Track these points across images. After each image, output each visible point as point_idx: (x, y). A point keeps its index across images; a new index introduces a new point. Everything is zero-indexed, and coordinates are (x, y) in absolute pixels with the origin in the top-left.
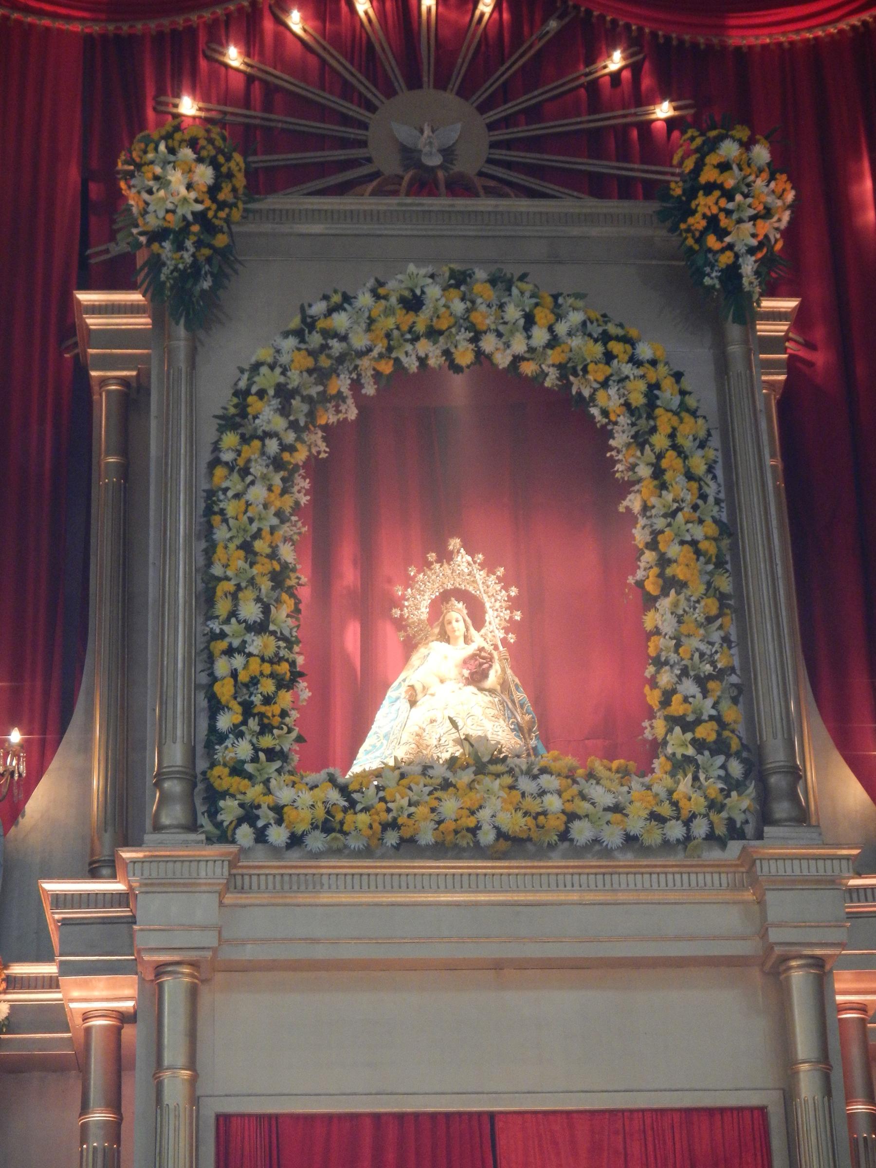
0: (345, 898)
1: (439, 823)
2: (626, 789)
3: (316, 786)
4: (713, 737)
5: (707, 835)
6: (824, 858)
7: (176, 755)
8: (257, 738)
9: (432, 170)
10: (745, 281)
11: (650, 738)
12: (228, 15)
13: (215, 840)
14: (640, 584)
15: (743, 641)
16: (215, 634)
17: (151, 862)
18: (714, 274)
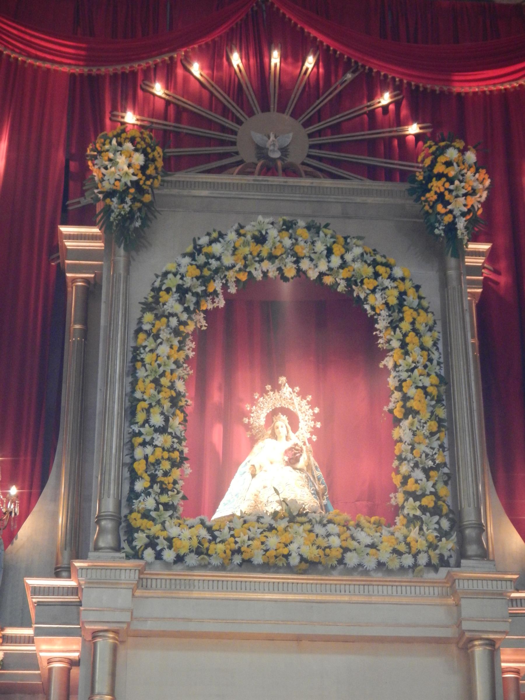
0: (208, 595)
1: (266, 551)
2: (379, 534)
3: (193, 527)
4: (432, 505)
5: (427, 563)
6: (497, 580)
7: (110, 505)
8: (159, 496)
9: (274, 160)
10: (459, 232)
11: (394, 504)
12: (156, 65)
13: (131, 557)
14: (391, 411)
15: (452, 447)
16: (136, 433)
17: (92, 569)
18: (441, 228)
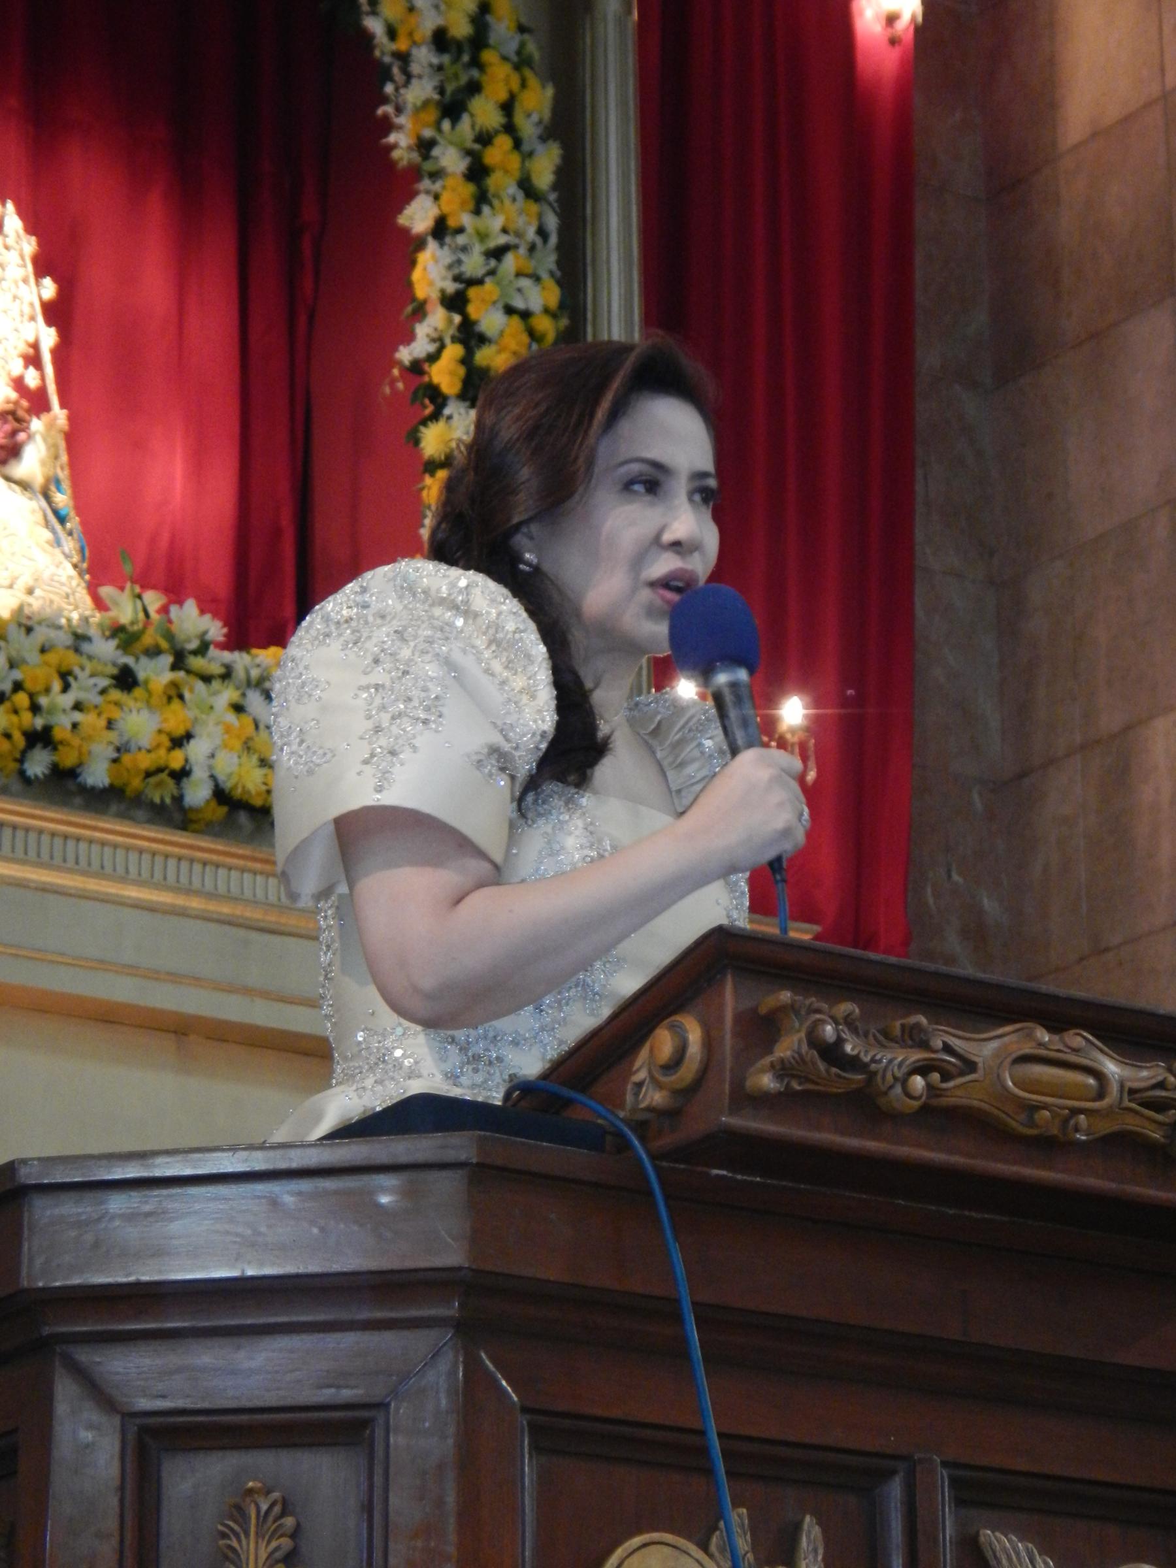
14: (417, 368)
